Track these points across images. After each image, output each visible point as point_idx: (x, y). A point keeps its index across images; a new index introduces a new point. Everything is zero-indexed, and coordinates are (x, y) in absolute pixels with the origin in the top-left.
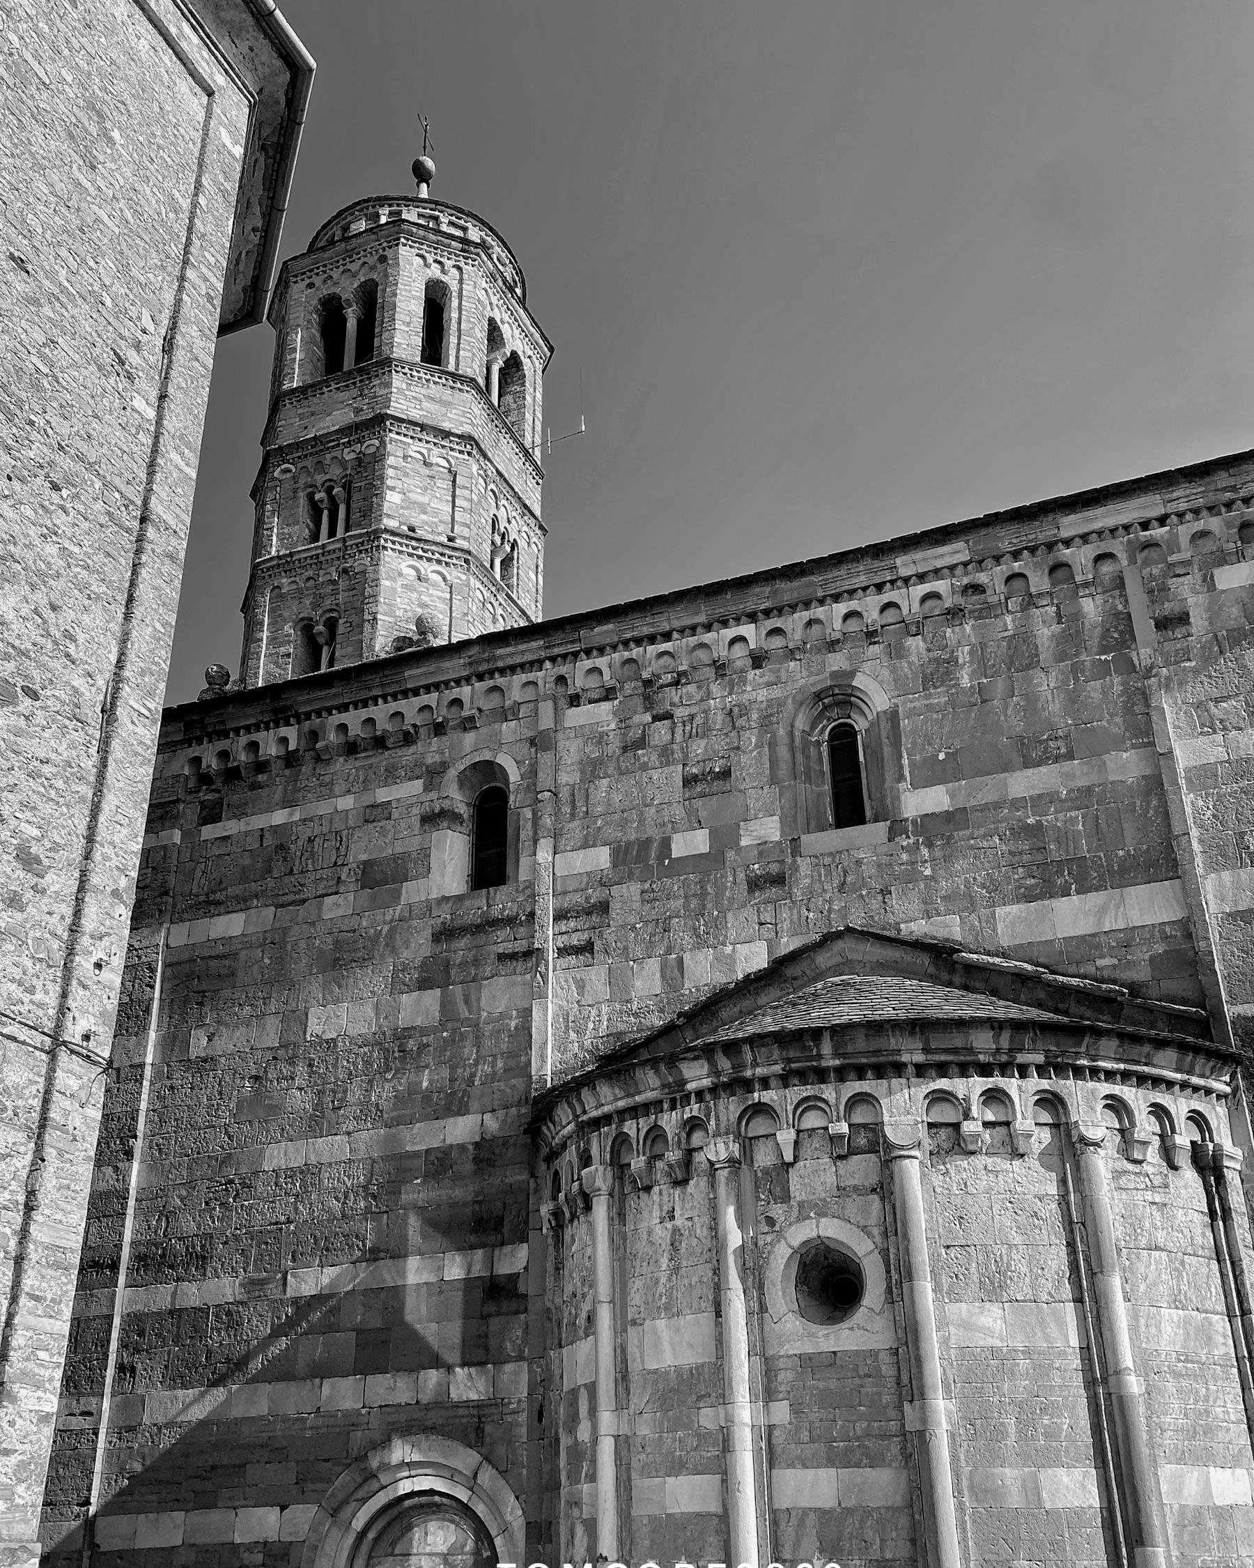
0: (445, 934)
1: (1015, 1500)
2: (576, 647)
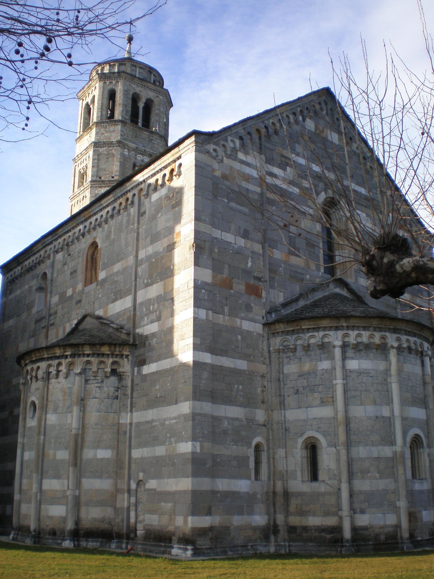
0: (38, 321)
1: (51, 457)
2: (56, 237)
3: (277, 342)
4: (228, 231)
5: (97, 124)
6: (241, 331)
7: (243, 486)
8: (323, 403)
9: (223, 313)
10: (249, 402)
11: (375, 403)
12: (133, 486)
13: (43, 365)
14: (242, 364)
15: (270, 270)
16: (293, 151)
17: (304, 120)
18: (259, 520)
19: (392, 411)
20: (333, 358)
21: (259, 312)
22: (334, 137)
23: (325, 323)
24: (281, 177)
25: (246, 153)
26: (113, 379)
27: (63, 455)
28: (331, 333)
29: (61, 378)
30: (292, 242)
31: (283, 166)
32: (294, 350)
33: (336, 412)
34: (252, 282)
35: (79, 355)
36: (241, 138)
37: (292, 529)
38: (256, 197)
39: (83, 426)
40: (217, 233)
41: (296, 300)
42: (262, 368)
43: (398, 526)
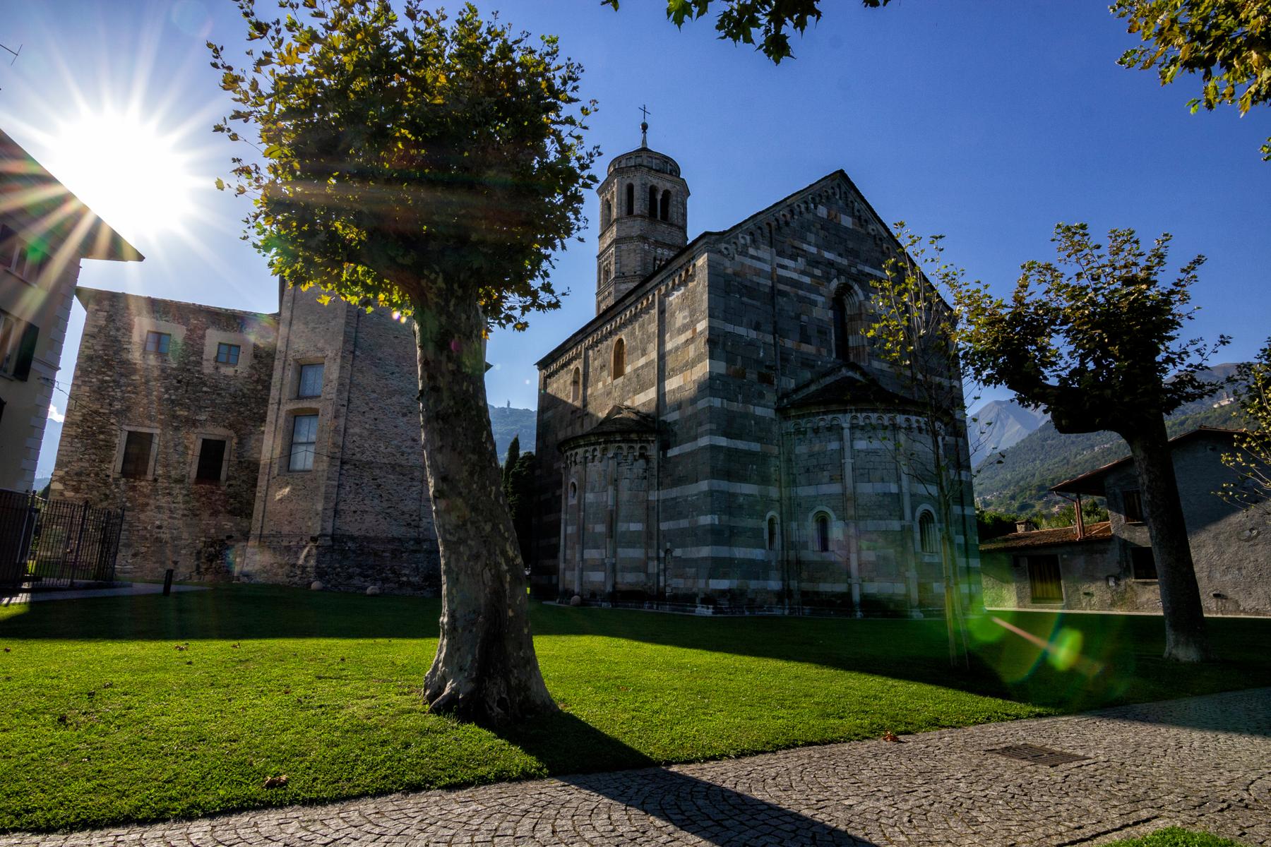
3: (790, 426)
4: (740, 325)
5: (617, 220)
6: (755, 417)
7: (757, 554)
8: (832, 480)
9: (737, 401)
10: (765, 480)
11: (883, 480)
12: (662, 554)
13: (580, 451)
14: (756, 447)
15: (782, 359)
16: (804, 240)
17: (816, 207)
18: (774, 585)
19: (900, 487)
20: (841, 439)
21: (771, 397)
22: (847, 221)
23: (834, 407)
24: (792, 269)
25: (757, 248)
26: (642, 462)
27: (600, 528)
28: (840, 416)
29: (596, 463)
30: (803, 330)
31: (793, 257)
32: (805, 433)
33: (845, 488)
34: (764, 371)
35: (611, 442)
36: (751, 234)
37: (805, 594)
38: (767, 290)
39: (617, 503)
40: (730, 328)
41: (807, 385)
42: (775, 450)
43: (907, 595)
